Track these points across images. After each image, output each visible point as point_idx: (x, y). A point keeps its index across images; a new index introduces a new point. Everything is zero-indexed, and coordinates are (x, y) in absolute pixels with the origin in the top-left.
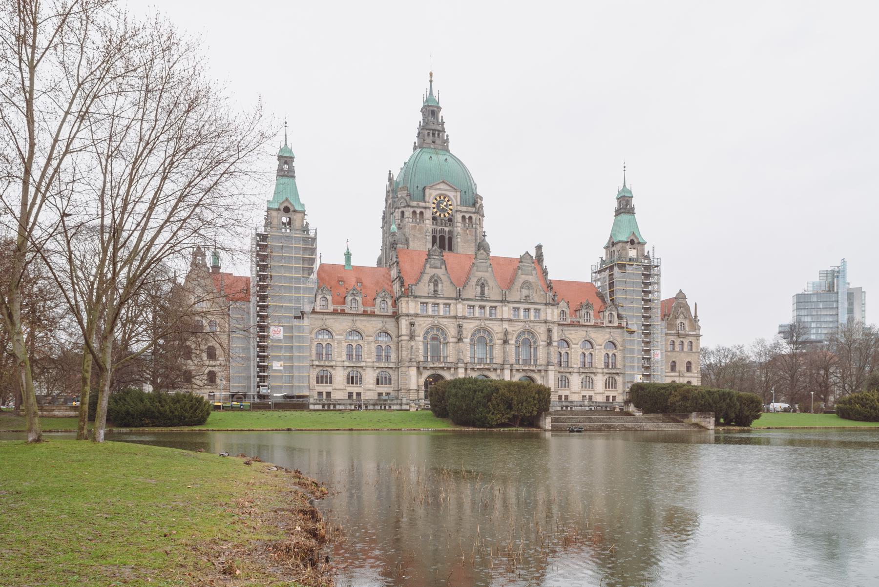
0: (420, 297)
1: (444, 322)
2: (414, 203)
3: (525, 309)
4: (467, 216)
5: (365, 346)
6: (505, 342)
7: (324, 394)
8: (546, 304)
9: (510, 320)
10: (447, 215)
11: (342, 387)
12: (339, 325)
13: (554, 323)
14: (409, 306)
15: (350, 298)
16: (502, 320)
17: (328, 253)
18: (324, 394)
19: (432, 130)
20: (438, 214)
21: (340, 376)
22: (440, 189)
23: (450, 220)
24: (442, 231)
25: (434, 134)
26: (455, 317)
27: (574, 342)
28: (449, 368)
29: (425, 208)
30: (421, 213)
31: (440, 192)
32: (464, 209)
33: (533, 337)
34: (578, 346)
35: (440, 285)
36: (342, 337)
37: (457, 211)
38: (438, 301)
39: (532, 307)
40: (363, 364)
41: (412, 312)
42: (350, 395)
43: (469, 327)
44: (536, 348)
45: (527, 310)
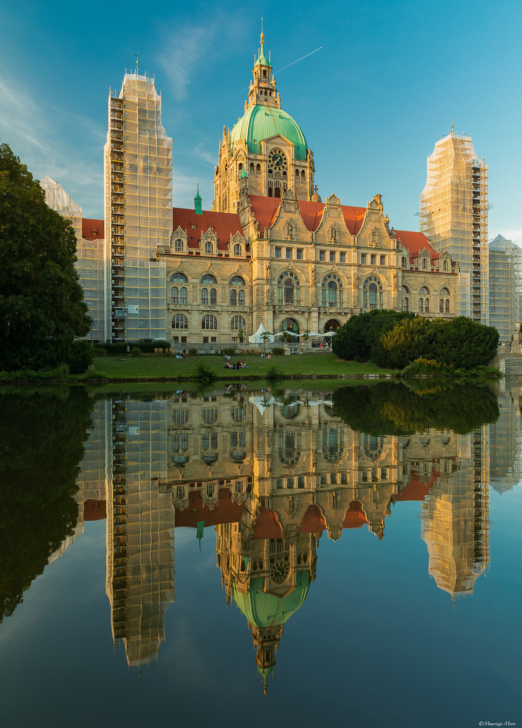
0: (275, 241)
4: (300, 170)
7: (180, 339)
10: (282, 168)
11: (197, 331)
15: (206, 241)
18: (180, 339)
21: (195, 320)
22: (275, 143)
23: (285, 173)
25: (266, 93)
27: (414, 288)
28: (303, 312)
30: (259, 166)
32: (298, 163)
34: (417, 292)
38: (291, 245)
39: (379, 253)
40: (218, 309)
41: (268, 256)
42: (206, 339)
44: (381, 293)
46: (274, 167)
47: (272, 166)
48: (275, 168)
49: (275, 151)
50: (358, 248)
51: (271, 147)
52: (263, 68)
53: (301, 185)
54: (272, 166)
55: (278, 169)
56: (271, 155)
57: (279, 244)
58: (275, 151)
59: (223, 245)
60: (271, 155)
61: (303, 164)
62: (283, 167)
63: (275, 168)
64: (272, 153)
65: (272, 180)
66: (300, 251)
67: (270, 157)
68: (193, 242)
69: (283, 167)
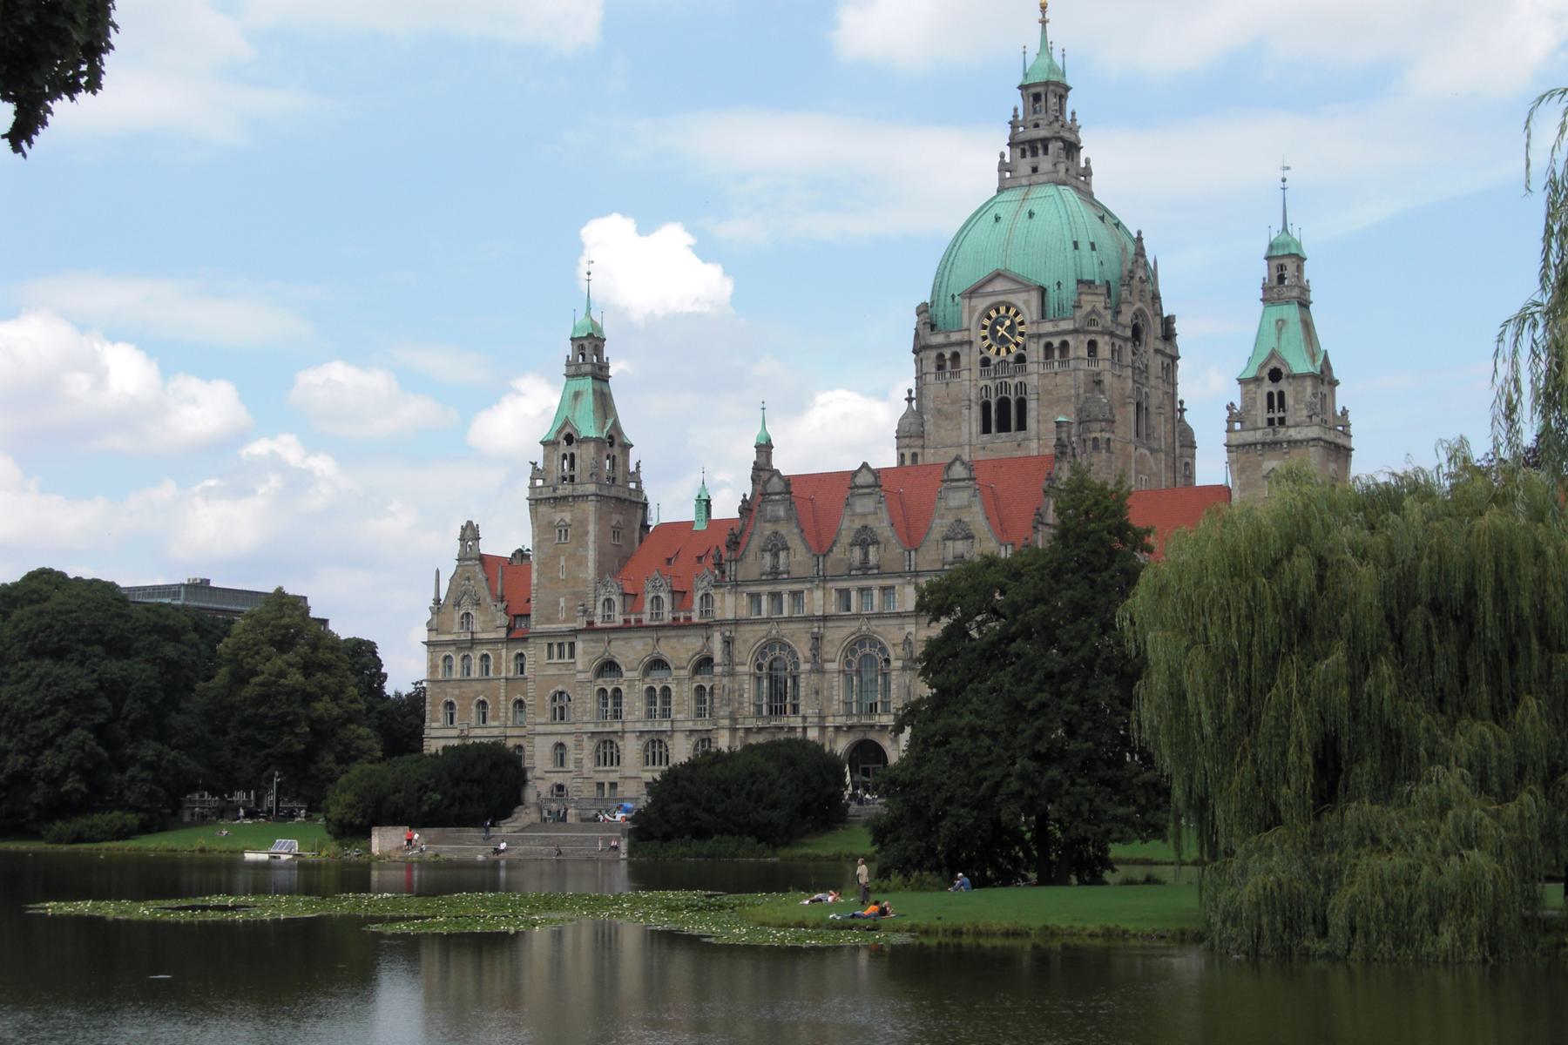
2: (939, 339)
3: (883, 589)
4: (1056, 342)
5: (673, 687)
7: (607, 786)
10: (1013, 348)
12: (631, 652)
15: (651, 596)
16: (899, 615)
17: (669, 503)
18: (607, 786)
19: (1044, 135)
20: (994, 349)
23: (1021, 359)
25: (1035, 154)
26: (807, 619)
29: (961, 344)
30: (956, 356)
31: (993, 300)
32: (1048, 327)
35: (782, 555)
36: (634, 675)
37: (1031, 336)
41: (730, 616)
43: (838, 635)
46: (994, 349)
47: (989, 347)
48: (998, 353)
49: (998, 311)
51: (981, 304)
52: (1033, 90)
53: (1058, 379)
54: (989, 347)
55: (1003, 351)
56: (987, 322)
57: (754, 589)
58: (998, 311)
59: (680, 596)
60: (987, 322)
61: (1066, 325)
62: (1017, 344)
63: (998, 353)
64: (989, 317)
65: (988, 382)
67: (984, 327)
68: (632, 598)
69: (1017, 344)
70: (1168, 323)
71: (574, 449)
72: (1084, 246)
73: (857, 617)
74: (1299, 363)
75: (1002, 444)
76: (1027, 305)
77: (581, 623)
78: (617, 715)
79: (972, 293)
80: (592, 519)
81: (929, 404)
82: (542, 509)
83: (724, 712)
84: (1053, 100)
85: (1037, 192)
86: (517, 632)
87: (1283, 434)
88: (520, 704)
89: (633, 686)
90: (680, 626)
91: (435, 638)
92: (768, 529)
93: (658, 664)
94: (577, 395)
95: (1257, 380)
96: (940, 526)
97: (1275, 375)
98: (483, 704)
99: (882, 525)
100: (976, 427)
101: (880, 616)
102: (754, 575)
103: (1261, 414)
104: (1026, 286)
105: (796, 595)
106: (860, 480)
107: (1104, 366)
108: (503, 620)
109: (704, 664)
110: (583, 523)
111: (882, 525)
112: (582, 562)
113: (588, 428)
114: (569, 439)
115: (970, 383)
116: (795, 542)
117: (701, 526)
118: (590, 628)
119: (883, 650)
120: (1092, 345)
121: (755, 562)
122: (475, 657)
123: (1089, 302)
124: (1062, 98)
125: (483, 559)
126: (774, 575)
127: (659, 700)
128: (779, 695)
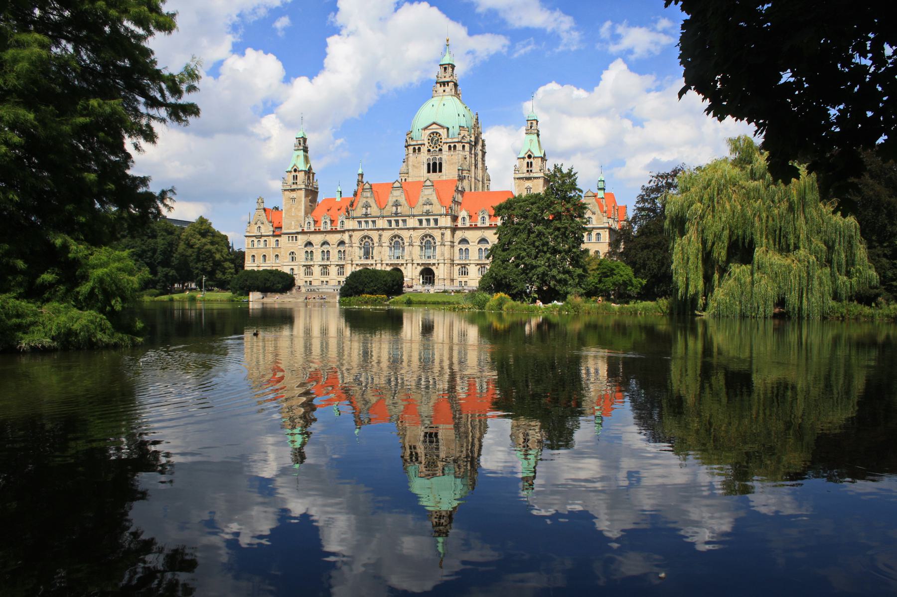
1: (370, 233)
2: (414, 143)
4: (452, 145)
6: (411, 245)
8: (441, 215)
9: (414, 229)
12: (317, 239)
13: (446, 228)
14: (350, 224)
21: (317, 270)
23: (440, 150)
24: (435, 158)
30: (419, 149)
33: (434, 239)
39: (431, 218)
43: (387, 235)
45: (428, 221)
50: (414, 216)
51: (428, 132)
66: (374, 222)
70: (483, 141)
71: (297, 173)
72: (461, 115)
73: (393, 229)
74: (537, 153)
75: (434, 176)
76: (443, 132)
77: (300, 230)
78: (312, 259)
79: (426, 128)
80: (303, 196)
81: (410, 163)
82: (287, 193)
83: (350, 258)
84: (450, 69)
85: (445, 98)
86: (277, 232)
87: (532, 175)
88: (277, 256)
89: (317, 251)
90: (332, 232)
91: (248, 234)
92: (364, 200)
93: (325, 243)
94: (298, 156)
95: (524, 158)
96: (421, 201)
97: (529, 157)
98: (264, 256)
99: (402, 200)
100: (426, 170)
101: (401, 229)
102: (359, 215)
103: (525, 169)
104: (442, 127)
105: (374, 222)
106: (395, 185)
107: (467, 153)
108: (272, 229)
109: (342, 243)
110: (300, 198)
111: (402, 200)
112: (300, 210)
113: (302, 166)
114: (295, 170)
115: (424, 157)
116: (373, 204)
117: (338, 199)
118: (303, 232)
119: (402, 239)
120: (464, 146)
121: (359, 211)
122: (262, 240)
123: (463, 133)
124: (453, 69)
125: (265, 210)
126: (366, 215)
127: (326, 254)
128: (367, 255)
